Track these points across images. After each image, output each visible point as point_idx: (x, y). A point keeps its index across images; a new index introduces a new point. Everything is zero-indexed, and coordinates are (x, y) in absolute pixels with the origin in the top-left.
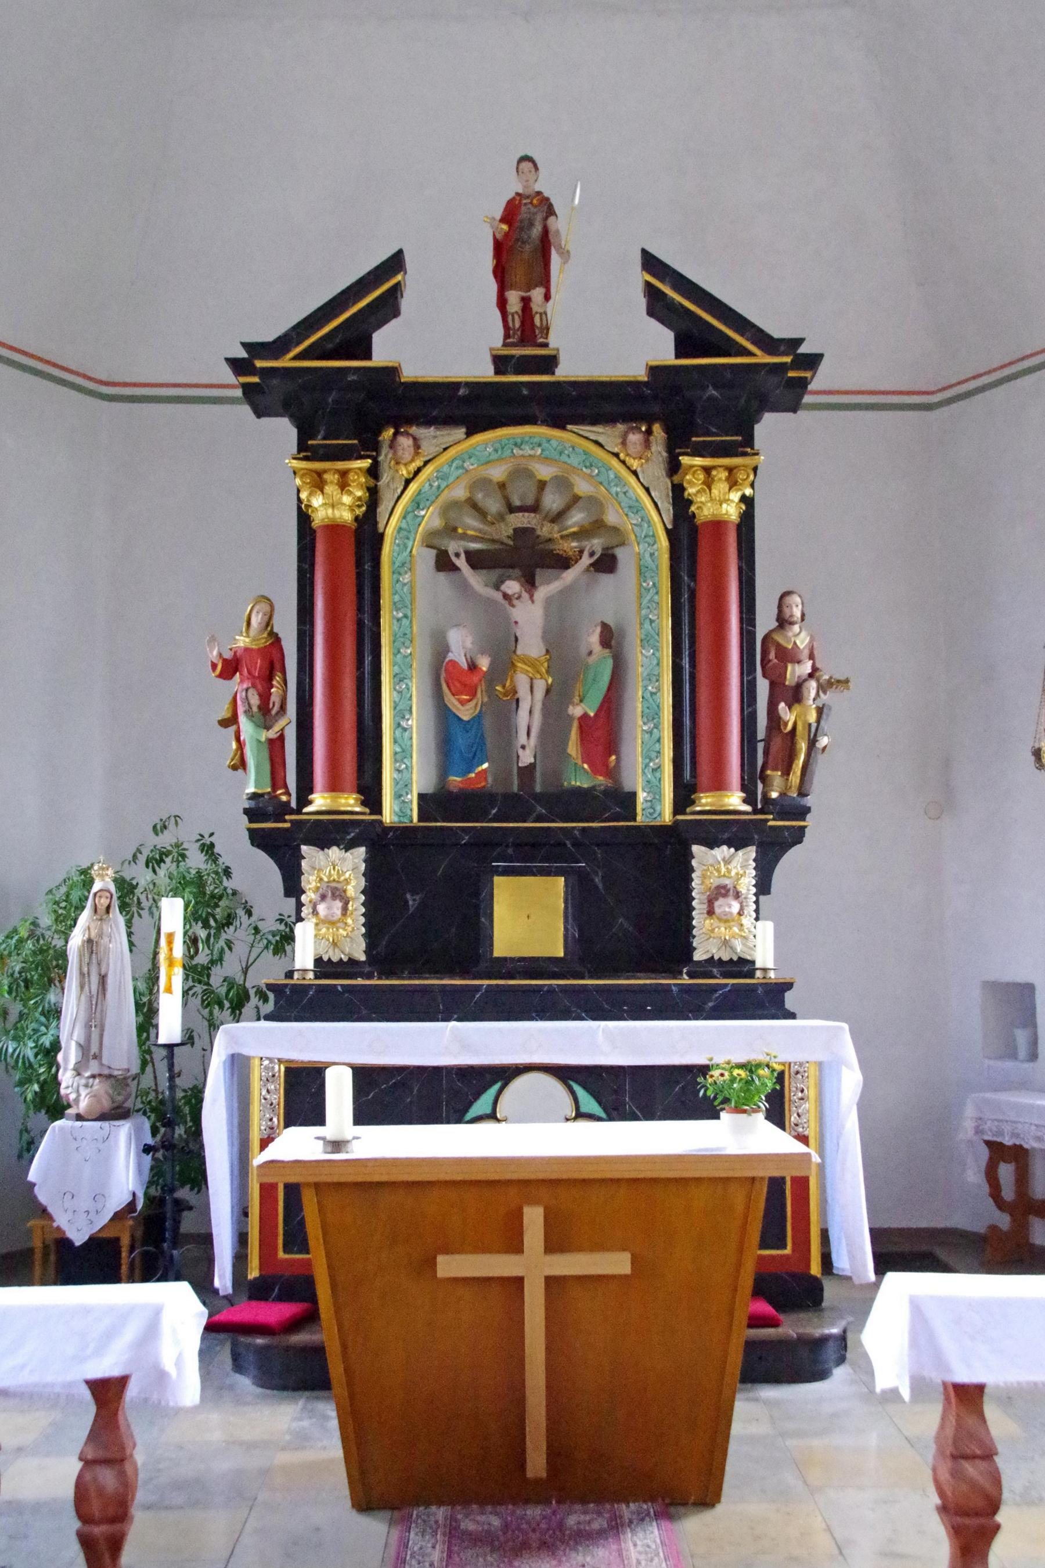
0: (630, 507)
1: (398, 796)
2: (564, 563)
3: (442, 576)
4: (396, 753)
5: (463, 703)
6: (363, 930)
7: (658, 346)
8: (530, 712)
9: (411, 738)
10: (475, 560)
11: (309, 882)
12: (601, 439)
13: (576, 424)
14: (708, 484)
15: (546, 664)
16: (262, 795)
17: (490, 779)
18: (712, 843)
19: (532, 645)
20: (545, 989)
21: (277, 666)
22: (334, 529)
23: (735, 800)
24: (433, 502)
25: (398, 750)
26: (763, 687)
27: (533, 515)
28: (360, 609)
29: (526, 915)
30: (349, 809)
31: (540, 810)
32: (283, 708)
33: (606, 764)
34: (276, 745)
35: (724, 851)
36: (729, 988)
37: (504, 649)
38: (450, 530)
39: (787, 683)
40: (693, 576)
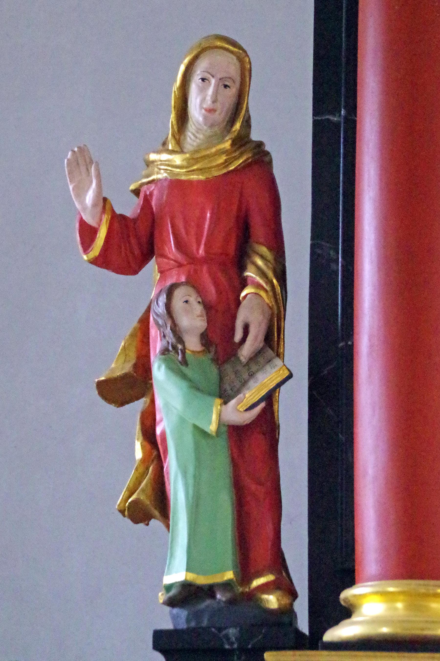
16: (209, 591)
21: (258, 229)
32: (273, 340)
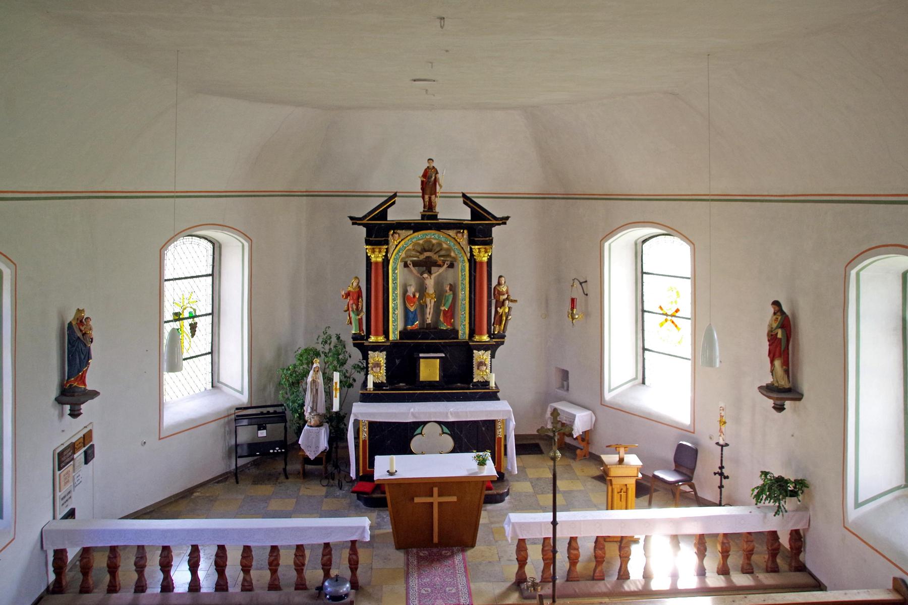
2: (440, 266)
7: (465, 214)
10: (415, 264)
11: (371, 361)
14: (479, 252)
19: (431, 290)
22: (377, 263)
23: (485, 338)
26: (494, 302)
29: (430, 369)
34: (360, 320)
35: (483, 352)
37: (422, 289)
38: (408, 256)
40: (475, 272)
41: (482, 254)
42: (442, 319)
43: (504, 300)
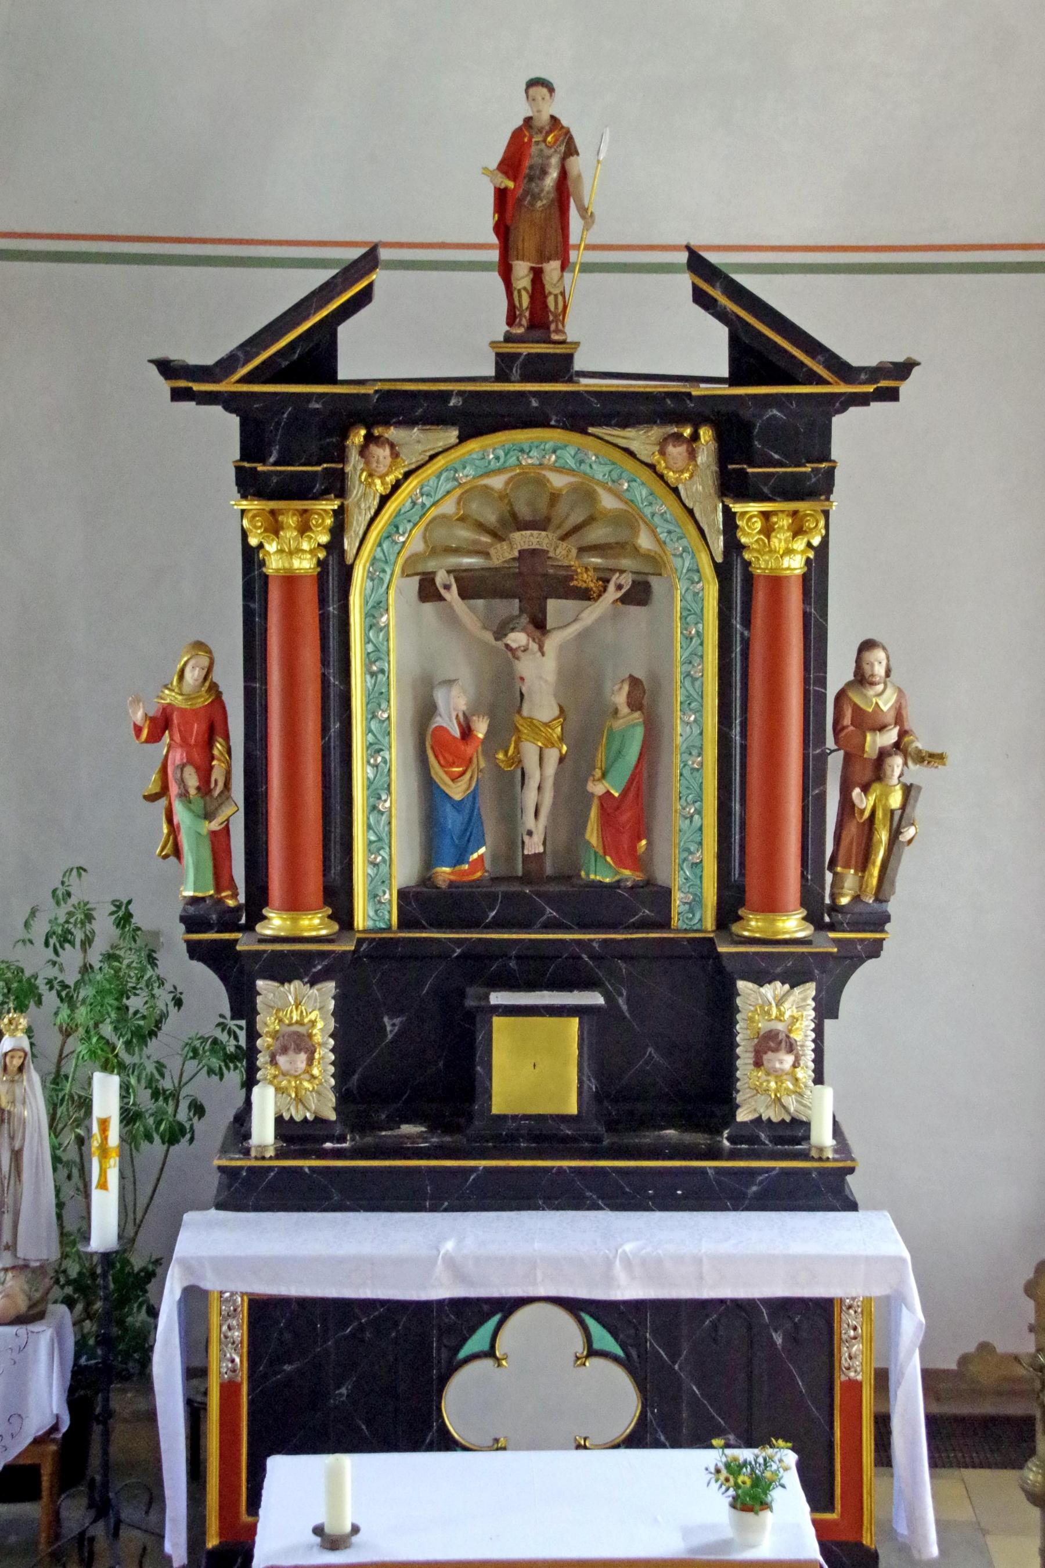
0: (669, 532)
1: (373, 896)
3: (428, 607)
4: (371, 842)
5: (455, 778)
6: (333, 1082)
8: (539, 788)
9: (390, 823)
10: (471, 586)
11: (267, 1022)
12: (634, 446)
13: (600, 425)
14: (768, 531)
15: (559, 729)
16: (203, 899)
17: (487, 865)
18: (761, 978)
19: (542, 706)
20: (554, 1171)
21: (218, 727)
23: (792, 924)
24: (415, 525)
25: (373, 838)
27: (544, 533)
28: (325, 662)
29: (535, 1062)
30: (314, 933)
31: (550, 912)
32: (227, 785)
33: (633, 848)
35: (778, 988)
36: (774, 1173)
37: (504, 699)
39: (865, 756)
40: (747, 622)
41: (779, 541)
42: (592, 836)
43: (883, 755)
